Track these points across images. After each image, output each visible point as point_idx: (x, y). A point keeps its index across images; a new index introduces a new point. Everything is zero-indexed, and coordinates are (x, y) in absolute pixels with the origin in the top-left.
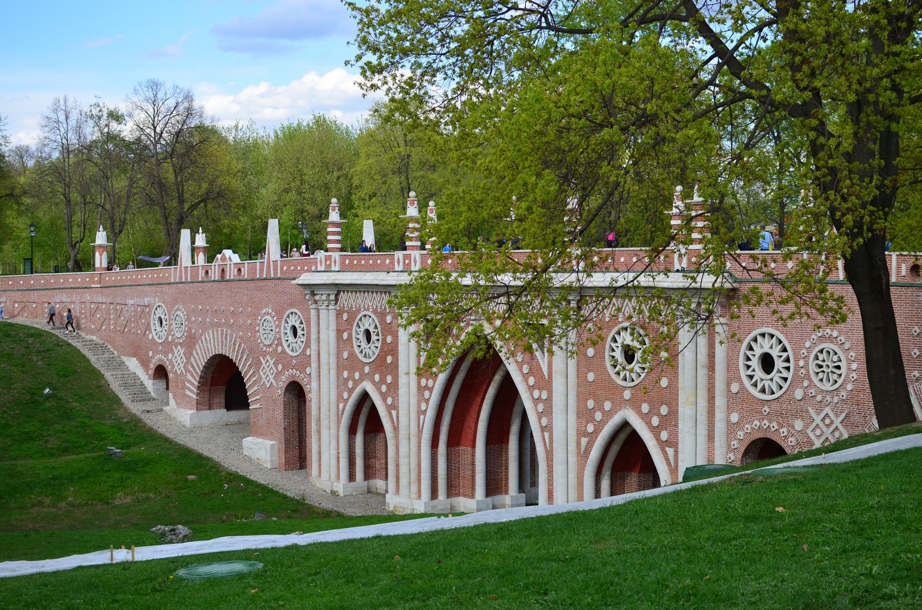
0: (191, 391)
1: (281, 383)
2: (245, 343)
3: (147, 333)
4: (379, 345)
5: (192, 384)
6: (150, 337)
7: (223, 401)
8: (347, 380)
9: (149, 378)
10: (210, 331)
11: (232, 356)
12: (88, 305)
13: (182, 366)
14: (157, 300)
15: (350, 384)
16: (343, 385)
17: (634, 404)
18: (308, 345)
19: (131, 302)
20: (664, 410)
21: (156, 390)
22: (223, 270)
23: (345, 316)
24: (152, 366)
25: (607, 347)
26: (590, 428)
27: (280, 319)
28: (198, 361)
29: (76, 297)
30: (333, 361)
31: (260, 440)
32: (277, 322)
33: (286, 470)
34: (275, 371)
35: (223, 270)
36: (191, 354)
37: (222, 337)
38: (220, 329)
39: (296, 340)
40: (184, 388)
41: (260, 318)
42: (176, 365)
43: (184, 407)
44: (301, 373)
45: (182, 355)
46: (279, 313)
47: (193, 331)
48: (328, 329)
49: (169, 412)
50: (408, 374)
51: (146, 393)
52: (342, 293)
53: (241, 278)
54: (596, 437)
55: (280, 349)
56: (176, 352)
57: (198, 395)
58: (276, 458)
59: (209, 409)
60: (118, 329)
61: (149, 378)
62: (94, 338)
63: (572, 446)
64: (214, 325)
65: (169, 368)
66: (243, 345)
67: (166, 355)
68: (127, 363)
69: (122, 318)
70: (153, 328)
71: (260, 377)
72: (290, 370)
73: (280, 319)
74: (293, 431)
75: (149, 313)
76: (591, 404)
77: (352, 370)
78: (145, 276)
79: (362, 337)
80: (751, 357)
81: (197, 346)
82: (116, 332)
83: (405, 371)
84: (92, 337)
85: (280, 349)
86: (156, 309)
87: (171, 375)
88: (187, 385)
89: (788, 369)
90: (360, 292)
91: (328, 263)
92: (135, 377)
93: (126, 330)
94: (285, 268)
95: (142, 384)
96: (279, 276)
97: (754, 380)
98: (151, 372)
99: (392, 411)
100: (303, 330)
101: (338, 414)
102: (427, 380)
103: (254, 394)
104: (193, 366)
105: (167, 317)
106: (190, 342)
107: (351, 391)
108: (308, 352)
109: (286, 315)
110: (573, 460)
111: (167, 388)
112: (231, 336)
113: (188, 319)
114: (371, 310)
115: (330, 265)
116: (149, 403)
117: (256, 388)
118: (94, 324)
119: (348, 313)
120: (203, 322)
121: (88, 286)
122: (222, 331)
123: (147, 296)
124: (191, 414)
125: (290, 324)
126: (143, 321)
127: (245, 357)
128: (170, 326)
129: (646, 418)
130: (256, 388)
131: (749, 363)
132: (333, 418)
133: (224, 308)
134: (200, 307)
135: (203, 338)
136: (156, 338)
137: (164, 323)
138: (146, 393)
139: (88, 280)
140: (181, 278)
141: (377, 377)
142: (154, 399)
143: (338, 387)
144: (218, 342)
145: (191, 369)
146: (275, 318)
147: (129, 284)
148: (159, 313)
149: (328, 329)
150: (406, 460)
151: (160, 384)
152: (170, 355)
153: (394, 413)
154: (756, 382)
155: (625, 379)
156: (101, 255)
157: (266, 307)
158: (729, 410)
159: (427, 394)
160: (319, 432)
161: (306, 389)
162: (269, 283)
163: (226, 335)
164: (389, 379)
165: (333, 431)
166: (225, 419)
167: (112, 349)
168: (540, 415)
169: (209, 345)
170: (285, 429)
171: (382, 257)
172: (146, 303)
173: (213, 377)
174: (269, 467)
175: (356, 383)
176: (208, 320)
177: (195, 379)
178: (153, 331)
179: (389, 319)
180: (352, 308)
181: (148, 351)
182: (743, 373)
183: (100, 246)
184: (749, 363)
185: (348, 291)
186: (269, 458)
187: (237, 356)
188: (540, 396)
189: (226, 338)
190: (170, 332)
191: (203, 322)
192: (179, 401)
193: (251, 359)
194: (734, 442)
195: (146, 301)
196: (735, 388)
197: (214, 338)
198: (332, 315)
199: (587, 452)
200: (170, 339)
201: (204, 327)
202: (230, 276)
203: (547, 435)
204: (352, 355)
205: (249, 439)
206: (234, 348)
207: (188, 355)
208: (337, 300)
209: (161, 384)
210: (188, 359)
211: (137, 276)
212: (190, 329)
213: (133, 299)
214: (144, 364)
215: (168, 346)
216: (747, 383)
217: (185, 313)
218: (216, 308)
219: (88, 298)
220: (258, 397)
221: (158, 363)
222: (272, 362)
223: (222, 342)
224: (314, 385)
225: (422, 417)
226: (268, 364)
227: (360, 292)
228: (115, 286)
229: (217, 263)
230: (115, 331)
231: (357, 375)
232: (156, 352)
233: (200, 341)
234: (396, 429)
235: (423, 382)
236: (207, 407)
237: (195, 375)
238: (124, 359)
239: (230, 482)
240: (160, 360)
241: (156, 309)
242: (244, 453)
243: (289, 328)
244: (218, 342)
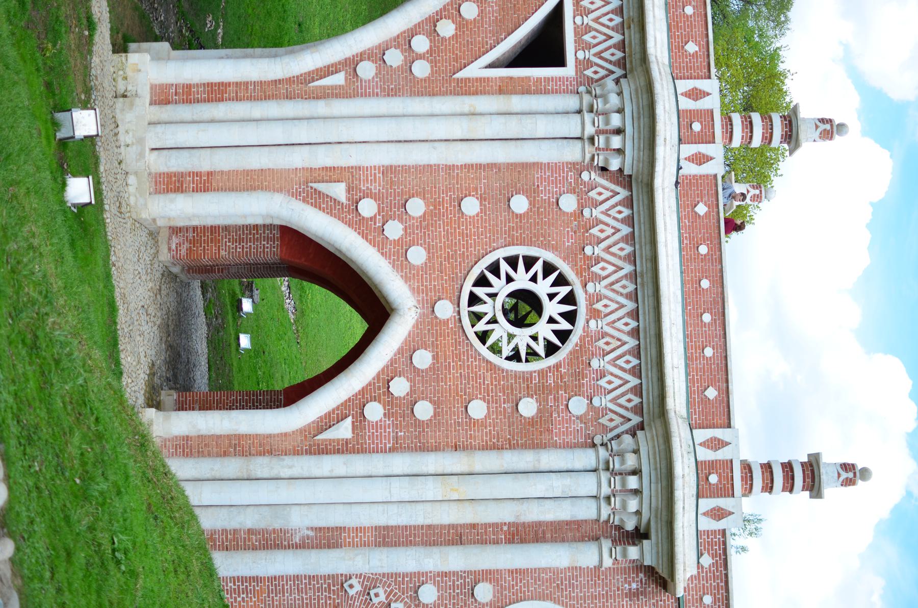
20: (424, 410)
25: (532, 251)
54: (350, 224)
63: (324, 158)
76: (416, 207)
110: (298, 159)
155: (474, 299)
158: (442, 578)
168: (377, 54)
188: (420, 57)
194: (382, 598)
199: (319, 201)
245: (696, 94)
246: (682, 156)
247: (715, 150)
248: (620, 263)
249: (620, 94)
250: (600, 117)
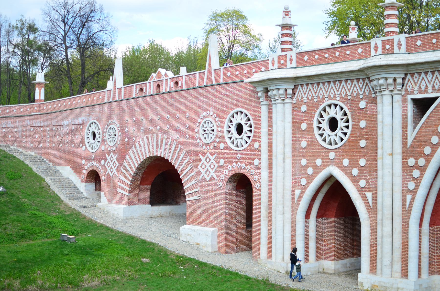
1: (223, 176)
2: (182, 144)
3: (81, 145)
4: (349, 131)
6: (84, 148)
8: (305, 168)
9: (82, 182)
10: (145, 138)
11: (168, 157)
12: (28, 129)
13: (114, 169)
14: (91, 118)
15: (310, 171)
16: (300, 172)
18: (258, 138)
19: (66, 123)
21: (88, 191)
22: (158, 86)
23: (304, 108)
24: (85, 172)
28: (131, 164)
29: (18, 123)
30: (289, 151)
31: (197, 227)
32: (219, 122)
33: (226, 253)
34: (216, 166)
35: (158, 86)
36: (124, 158)
37: (157, 142)
38: (155, 135)
40: (116, 187)
41: (199, 120)
42: (108, 169)
43: (116, 203)
44: (246, 165)
45: (115, 160)
46: (221, 115)
47: (127, 139)
48: (284, 121)
49: (101, 207)
50: (392, 154)
51: (79, 193)
52: (300, 87)
53: (178, 89)
56: (108, 158)
57: (130, 192)
58: (216, 243)
60: (54, 145)
61: (82, 182)
62: (33, 153)
64: (147, 132)
65: (101, 172)
66: (180, 146)
67: (99, 161)
68: (61, 171)
69: (58, 137)
70: (86, 140)
72: (234, 164)
73: (222, 119)
74: (232, 219)
75: (83, 130)
77: (311, 157)
78: (79, 101)
79: (325, 125)
81: (131, 152)
82: (51, 148)
83: (390, 151)
84: (31, 153)
85: (222, 146)
86: (90, 126)
87: (103, 178)
89: (347, 127)
90: (324, 83)
91: (282, 62)
92: (70, 182)
93: (61, 145)
94: (229, 74)
95: (75, 187)
96: (222, 81)
98: (84, 177)
99: (366, 193)
101: (293, 200)
102: (417, 159)
103: (190, 188)
107: (310, 178)
108: (256, 145)
112: (168, 139)
113: (122, 130)
114: (338, 99)
115: (285, 63)
116: (83, 201)
117: (193, 182)
118: (33, 143)
119: (307, 105)
120: (138, 131)
121: (29, 114)
122: (158, 136)
123: (81, 116)
124: (124, 208)
126: (77, 137)
127: (182, 156)
128: (104, 137)
130: (193, 182)
132: (288, 204)
133: (159, 117)
134: (134, 119)
135: (137, 144)
136: (89, 149)
138: (79, 193)
139: (28, 109)
140: (114, 97)
141: (346, 162)
142: (86, 198)
143: (293, 175)
144: (153, 146)
145: (124, 171)
146: (217, 119)
147: (65, 109)
148: (93, 128)
149: (284, 121)
150: (390, 240)
151: (91, 186)
152: (103, 162)
153: (369, 195)
156: (40, 90)
157: (206, 111)
159: (416, 173)
161: (253, 179)
162: (210, 89)
163: (162, 139)
164: (362, 162)
165: (288, 215)
166: (150, 212)
167: (48, 162)
169: (143, 149)
170: (226, 216)
171: (353, 48)
172: (81, 122)
173: (142, 177)
174: (210, 251)
175: (318, 170)
176: (142, 128)
178: (86, 144)
179: (362, 104)
180: (313, 98)
181: (82, 160)
183: (40, 83)
185: (307, 85)
186: (209, 243)
187: (173, 156)
189: (162, 142)
191: (138, 131)
192: (110, 198)
193: (188, 157)
195: (80, 120)
197: (148, 143)
198: (288, 108)
201: (138, 135)
202: (166, 89)
204: (312, 144)
205: (186, 226)
206: (170, 150)
207: (121, 160)
208: (294, 94)
209: (92, 186)
210: (121, 164)
211: (72, 102)
212: (123, 139)
213: (67, 120)
214: (77, 170)
217: (118, 125)
218: (151, 117)
219: (29, 123)
220: (196, 190)
221: (91, 169)
222: (212, 159)
223: (157, 145)
224: (265, 174)
225: (409, 197)
226: (208, 160)
227: (324, 83)
228: (51, 113)
229: (153, 80)
230: (51, 147)
231: (319, 162)
233: (133, 147)
235: (411, 162)
236: (137, 203)
237: (128, 176)
238: (58, 168)
239: (183, 264)
240: (92, 166)
242: (182, 239)
244: (153, 146)
245: (376, 48)
246: (398, 52)
247: (396, 38)
248: (421, 78)
249: (379, 79)
250: (389, 87)
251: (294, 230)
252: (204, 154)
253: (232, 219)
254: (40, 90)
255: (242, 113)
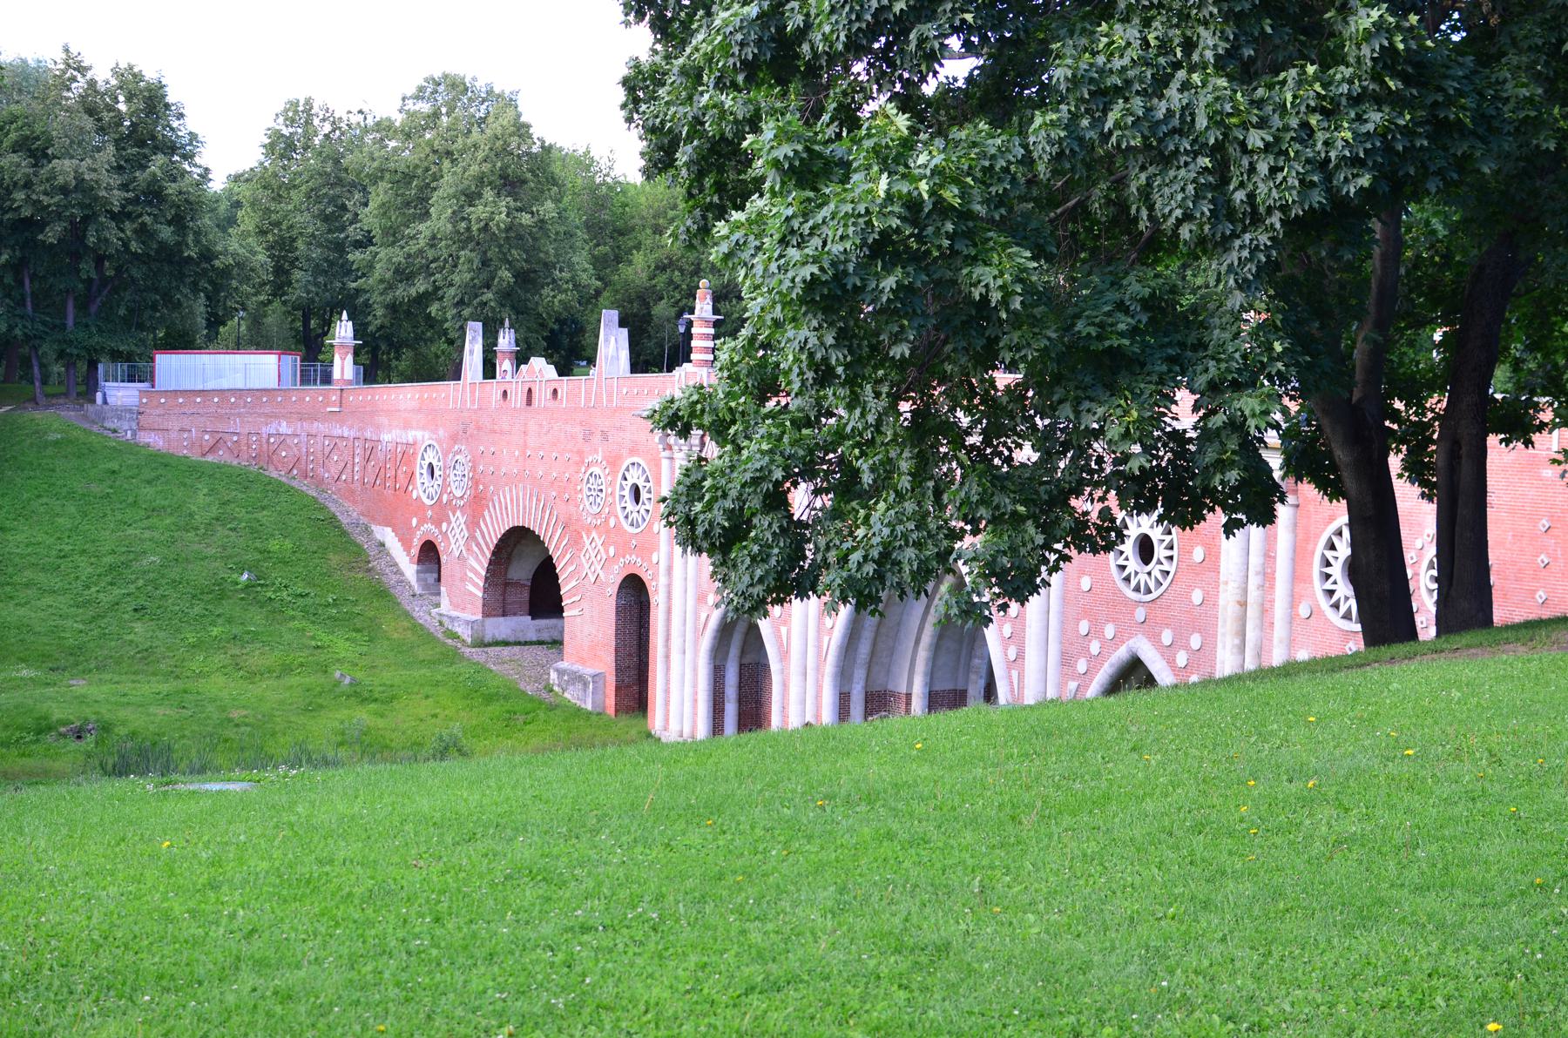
0: (475, 585)
3: (410, 488)
5: (476, 573)
6: (414, 496)
7: (526, 607)
13: (462, 542)
17: (1150, 628)
20: (1195, 641)
22: (530, 390)
24: (417, 543)
26: (1082, 666)
27: (614, 473)
35: (530, 390)
39: (638, 508)
42: (453, 541)
45: (463, 526)
54: (1091, 681)
55: (612, 522)
56: (453, 520)
57: (485, 590)
59: (504, 615)
65: (441, 548)
67: (438, 524)
70: (419, 482)
71: (581, 565)
73: (614, 473)
80: (1332, 561)
81: (486, 513)
85: (612, 522)
86: (425, 450)
87: (444, 558)
88: (470, 575)
97: (1335, 598)
98: (415, 551)
100: (649, 492)
101: (696, 629)
104: (478, 545)
105: (441, 464)
106: (477, 504)
109: (624, 467)
111: (439, 580)
125: (630, 482)
129: (1168, 653)
131: (1328, 570)
132: (689, 636)
135: (496, 498)
137: (437, 473)
145: (476, 549)
146: (607, 471)
148: (431, 457)
152: (444, 526)
153: (784, 630)
154: (1339, 600)
155: (1137, 589)
156: (343, 359)
160: (667, 657)
177: (480, 563)
178: (419, 485)
182: (1318, 586)
183: (342, 346)
184: (1328, 570)
190: (445, 486)
196: (1303, 611)
200: (445, 498)
203: (1015, 674)
207: (473, 524)
210: (472, 537)
215: (441, 512)
216: (1324, 604)
224: (663, 580)
232: (421, 522)
234: (784, 655)
241: (425, 450)
243: (627, 489)
251: (695, 686)
252: (588, 534)
253: (630, 655)
254: (343, 359)
255: (639, 465)
